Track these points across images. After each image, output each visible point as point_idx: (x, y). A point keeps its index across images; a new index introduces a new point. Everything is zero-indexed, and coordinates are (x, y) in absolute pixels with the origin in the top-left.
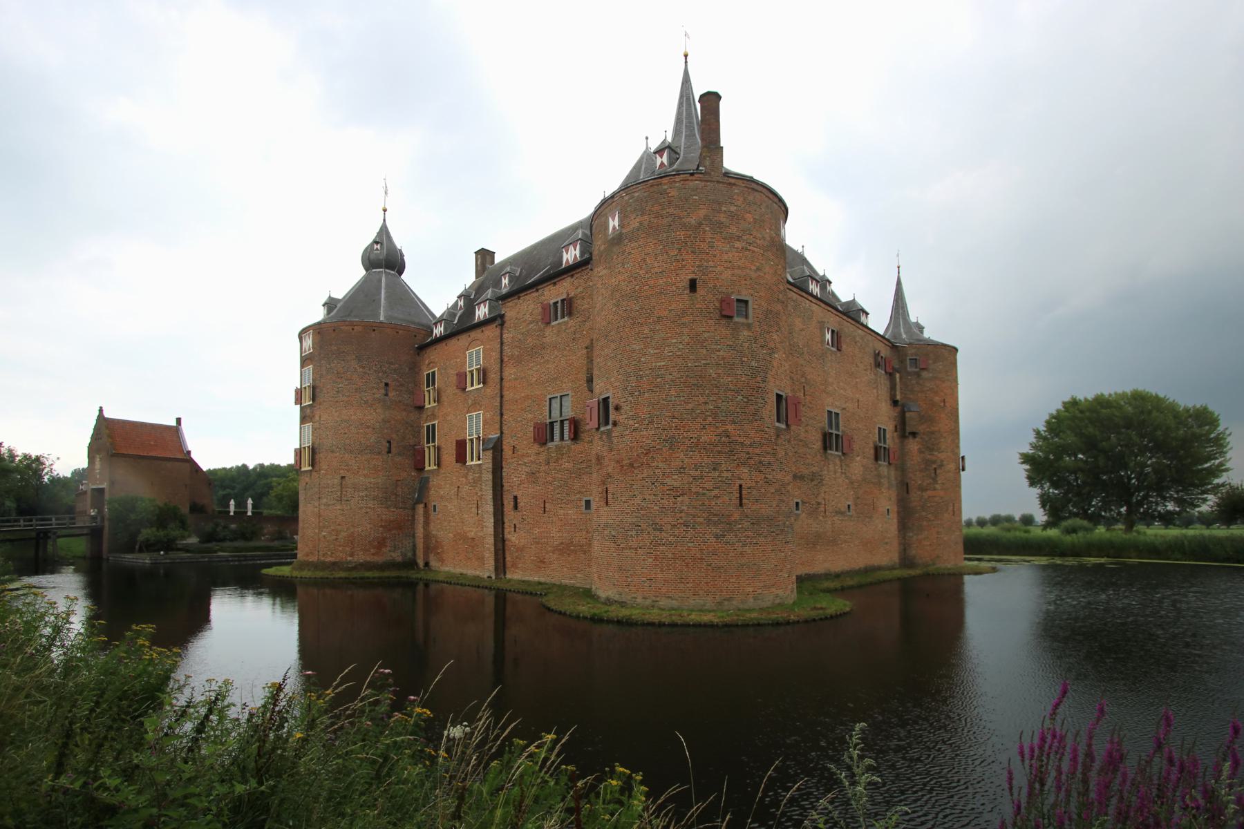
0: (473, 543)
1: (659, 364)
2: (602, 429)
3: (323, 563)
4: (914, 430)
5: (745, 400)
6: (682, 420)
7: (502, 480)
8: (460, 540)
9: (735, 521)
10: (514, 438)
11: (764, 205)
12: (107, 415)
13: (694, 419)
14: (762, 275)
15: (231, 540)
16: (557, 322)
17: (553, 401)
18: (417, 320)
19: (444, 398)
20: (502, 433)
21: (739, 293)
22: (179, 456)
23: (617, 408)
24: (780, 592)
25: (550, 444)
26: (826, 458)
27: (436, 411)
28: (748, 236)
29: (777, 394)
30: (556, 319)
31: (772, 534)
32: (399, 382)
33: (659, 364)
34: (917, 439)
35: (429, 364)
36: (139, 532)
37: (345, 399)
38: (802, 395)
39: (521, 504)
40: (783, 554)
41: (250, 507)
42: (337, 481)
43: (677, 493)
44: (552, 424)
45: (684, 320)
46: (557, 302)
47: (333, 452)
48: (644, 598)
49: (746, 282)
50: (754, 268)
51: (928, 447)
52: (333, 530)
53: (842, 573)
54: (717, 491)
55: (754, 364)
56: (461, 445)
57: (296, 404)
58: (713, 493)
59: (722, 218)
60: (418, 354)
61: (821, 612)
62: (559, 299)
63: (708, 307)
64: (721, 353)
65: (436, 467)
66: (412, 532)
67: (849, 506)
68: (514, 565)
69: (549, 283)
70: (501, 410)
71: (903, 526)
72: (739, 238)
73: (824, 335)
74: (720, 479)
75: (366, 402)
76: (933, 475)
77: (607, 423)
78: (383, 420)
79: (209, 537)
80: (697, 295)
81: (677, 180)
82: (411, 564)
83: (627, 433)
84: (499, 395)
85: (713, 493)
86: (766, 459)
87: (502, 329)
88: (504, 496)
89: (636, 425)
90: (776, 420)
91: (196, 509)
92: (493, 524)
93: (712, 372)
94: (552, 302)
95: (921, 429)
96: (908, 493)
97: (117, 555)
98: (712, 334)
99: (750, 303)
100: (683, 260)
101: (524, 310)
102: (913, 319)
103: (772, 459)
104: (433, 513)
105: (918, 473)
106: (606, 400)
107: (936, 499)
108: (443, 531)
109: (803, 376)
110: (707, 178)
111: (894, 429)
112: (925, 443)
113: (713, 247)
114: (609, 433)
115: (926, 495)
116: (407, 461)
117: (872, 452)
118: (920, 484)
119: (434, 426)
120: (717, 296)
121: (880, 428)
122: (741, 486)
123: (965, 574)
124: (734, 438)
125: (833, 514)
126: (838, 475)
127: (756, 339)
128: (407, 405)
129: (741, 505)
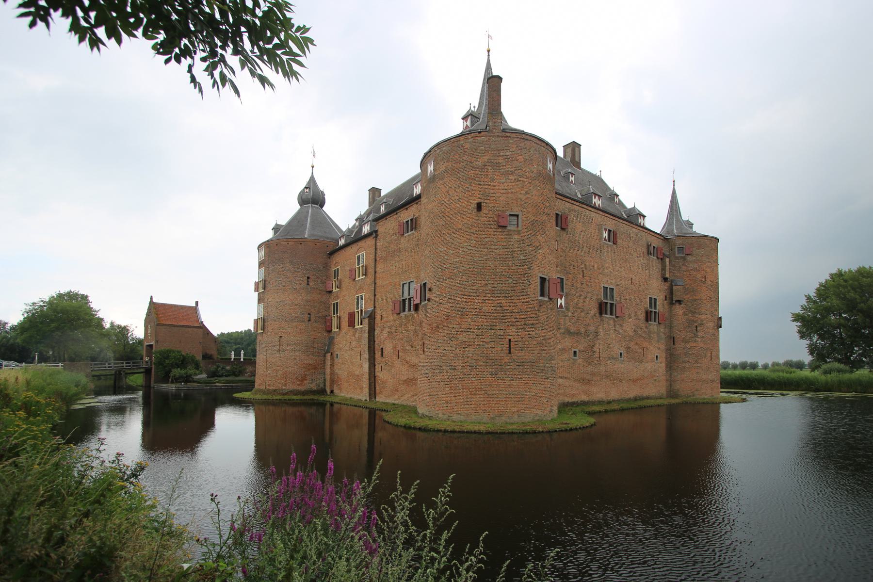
0: (358, 378)
1: (455, 260)
2: (422, 303)
3: (268, 390)
5: (515, 282)
6: (470, 296)
7: (374, 338)
8: (351, 376)
9: (505, 363)
10: (382, 310)
11: (533, 149)
12: (155, 300)
13: (478, 296)
14: (530, 196)
15: (226, 376)
16: (408, 234)
17: (405, 285)
18: (329, 236)
19: (343, 285)
20: (375, 307)
22: (196, 325)
23: (430, 290)
24: (540, 412)
25: (402, 314)
26: (601, 320)
27: (339, 294)
29: (540, 277)
30: (408, 232)
31: (534, 372)
32: (316, 276)
33: (455, 260)
35: (336, 264)
36: (170, 371)
37: (283, 288)
38: (581, 277)
39: (385, 353)
40: (542, 386)
41: (242, 355)
42: (277, 339)
43: (465, 345)
44: (404, 301)
45: (473, 230)
46: (408, 221)
47: (275, 321)
48: (443, 414)
49: (517, 202)
50: (523, 192)
52: (274, 370)
53: (614, 401)
54: (492, 344)
55: (522, 257)
56: (352, 316)
57: (255, 291)
58: (490, 345)
60: (329, 258)
61: (564, 426)
62: (409, 219)
65: (338, 330)
66: (323, 371)
68: (381, 392)
69: (404, 209)
70: (374, 293)
74: (495, 335)
75: (295, 289)
77: (425, 301)
79: (214, 374)
80: (481, 212)
81: (469, 137)
82: (322, 391)
83: (436, 306)
84: (373, 283)
85: (490, 345)
87: (376, 240)
88: (376, 348)
89: (441, 301)
90: (539, 295)
91: (206, 357)
92: (368, 366)
93: (491, 264)
94: (405, 221)
95: (686, 297)
97: (159, 385)
98: (492, 239)
99: (519, 216)
100: (472, 190)
101: (389, 226)
104: (336, 359)
106: (425, 284)
108: (341, 371)
111: (664, 298)
114: (426, 306)
116: (321, 326)
119: (337, 303)
120: (495, 213)
122: (510, 340)
123: (721, 403)
127: (523, 241)
129: (510, 352)
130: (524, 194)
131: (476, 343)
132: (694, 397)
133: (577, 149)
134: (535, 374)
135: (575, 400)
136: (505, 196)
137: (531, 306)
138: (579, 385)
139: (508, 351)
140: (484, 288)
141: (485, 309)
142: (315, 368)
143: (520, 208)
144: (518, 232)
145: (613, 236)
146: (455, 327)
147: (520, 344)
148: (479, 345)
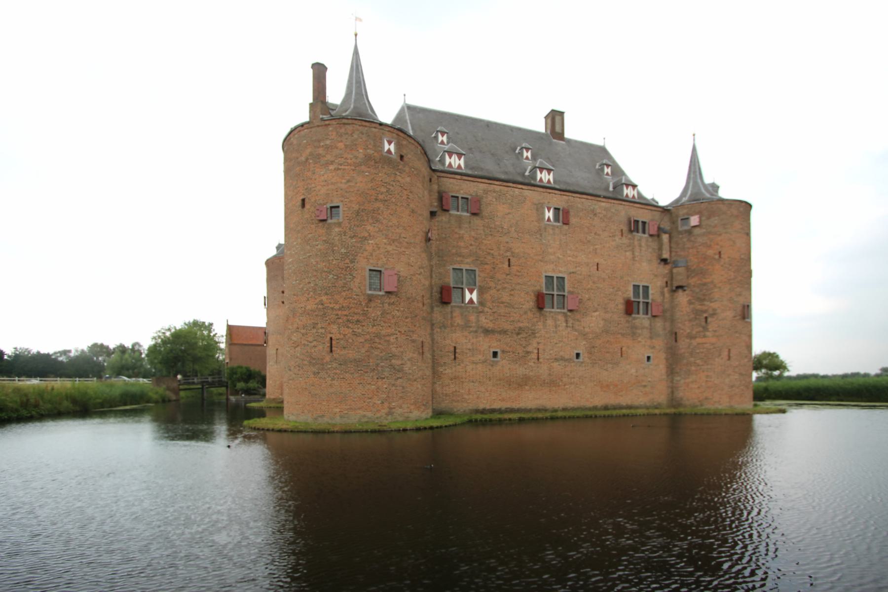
4: (681, 284)
5: (335, 277)
6: (297, 296)
9: (327, 363)
13: (303, 294)
21: (332, 201)
28: (339, 159)
34: (687, 292)
54: (315, 343)
55: (343, 251)
59: (321, 151)
63: (311, 217)
67: (578, 355)
72: (332, 163)
73: (543, 214)
76: (703, 324)
85: (313, 344)
86: (356, 317)
103: (361, 318)
105: (686, 323)
107: (705, 346)
109: (507, 251)
113: (314, 173)
115: (694, 342)
117: (622, 307)
118: (689, 333)
121: (636, 287)
122: (331, 339)
124: (326, 305)
125: (552, 361)
126: (561, 328)
127: (345, 233)
129: (331, 351)
130: (346, 183)
131: (303, 343)
132: (703, 407)
133: (558, 118)
134: (361, 373)
135: (496, 406)
136: (325, 188)
137: (356, 301)
138: (502, 390)
139: (329, 349)
141: (309, 307)
143: (340, 199)
144: (339, 224)
147: (342, 342)
148: (304, 345)
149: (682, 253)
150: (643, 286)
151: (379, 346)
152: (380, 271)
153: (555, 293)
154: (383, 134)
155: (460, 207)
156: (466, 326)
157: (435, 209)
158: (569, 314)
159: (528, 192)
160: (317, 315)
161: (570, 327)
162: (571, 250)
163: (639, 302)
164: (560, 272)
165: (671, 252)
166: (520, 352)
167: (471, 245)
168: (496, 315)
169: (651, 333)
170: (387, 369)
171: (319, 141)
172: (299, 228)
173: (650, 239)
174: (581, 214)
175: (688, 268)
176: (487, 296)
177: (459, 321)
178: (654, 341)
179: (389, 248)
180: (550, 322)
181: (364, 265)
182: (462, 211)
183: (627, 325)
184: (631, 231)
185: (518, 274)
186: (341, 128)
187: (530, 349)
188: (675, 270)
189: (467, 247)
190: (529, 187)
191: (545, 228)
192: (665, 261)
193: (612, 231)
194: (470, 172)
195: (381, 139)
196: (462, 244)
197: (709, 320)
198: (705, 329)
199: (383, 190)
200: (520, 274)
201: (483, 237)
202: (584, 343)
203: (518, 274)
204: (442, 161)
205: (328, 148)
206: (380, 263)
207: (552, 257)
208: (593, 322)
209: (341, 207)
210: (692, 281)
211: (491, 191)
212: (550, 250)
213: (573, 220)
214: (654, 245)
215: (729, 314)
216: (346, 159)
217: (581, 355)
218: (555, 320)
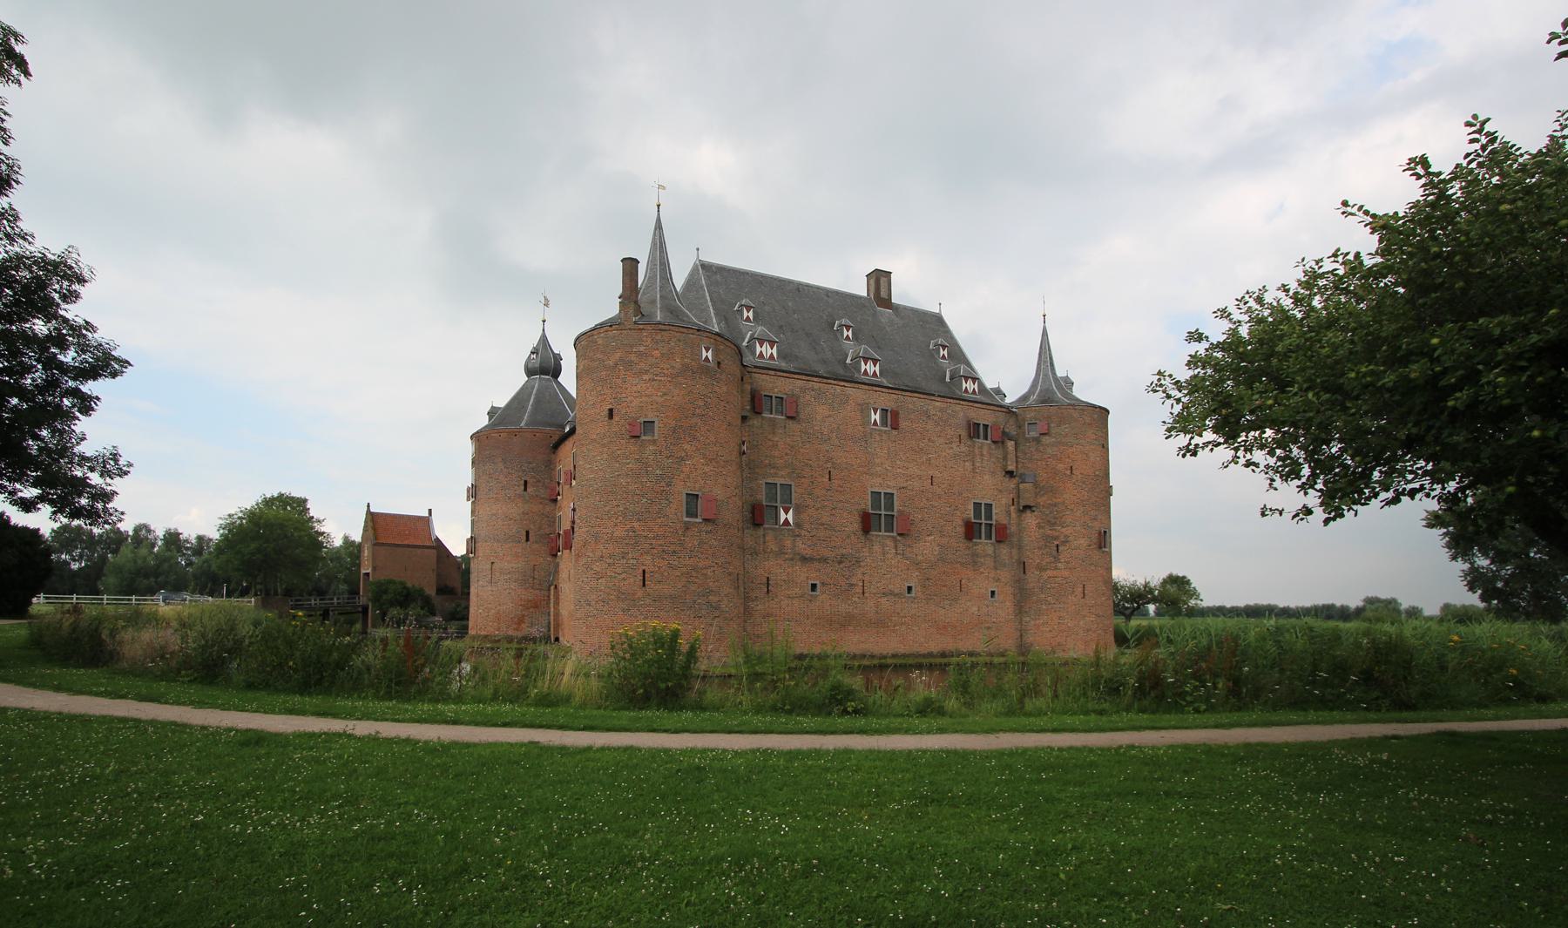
4: (1028, 503)
9: (639, 598)
34: (1036, 513)
42: (489, 566)
43: (599, 576)
51: (1049, 521)
54: (623, 576)
55: (658, 472)
58: (623, 576)
59: (633, 357)
64: (630, 465)
67: (910, 589)
71: (1020, 610)
72: (647, 372)
73: (870, 416)
75: (509, 498)
76: (1055, 553)
78: (523, 513)
85: (623, 576)
86: (672, 548)
96: (1024, 572)
102: (1060, 373)
103: (678, 548)
110: (622, 327)
112: (1044, 517)
117: (961, 530)
121: (977, 506)
122: (644, 571)
126: (890, 556)
128: (543, 498)
129: (644, 585)
130: (661, 396)
140: (616, 509)
142: (536, 607)
144: (654, 442)
145: (892, 419)
146: (591, 555)
149: (1030, 465)
150: (985, 504)
151: (697, 580)
152: (697, 495)
153: (883, 512)
154: (701, 340)
155: (774, 409)
156: (781, 553)
157: (745, 414)
158: (899, 538)
159: (851, 391)
160: (627, 544)
161: (899, 554)
162: (901, 459)
163: (981, 524)
164: (888, 487)
165: (1017, 462)
166: (843, 584)
167: (787, 454)
168: (814, 539)
169: (995, 562)
170: (704, 607)
171: (632, 346)
172: (605, 441)
173: (993, 446)
174: (912, 417)
175: (1036, 484)
176: (804, 516)
177: (773, 546)
178: (998, 572)
179: (707, 469)
180: (877, 548)
181: (681, 490)
182: (776, 414)
183: (967, 552)
184: (970, 437)
185: (839, 489)
186: (657, 334)
187: (854, 581)
188: (1021, 486)
189: (781, 457)
190: (852, 385)
191: (871, 434)
192: (1010, 474)
193: (949, 437)
194: (784, 365)
195: (699, 346)
196: (776, 453)
197: (1061, 548)
198: (1057, 559)
199: (701, 403)
200: (842, 489)
201: (800, 445)
202: (917, 573)
203: (839, 489)
204: (751, 348)
205: (640, 354)
206: (697, 486)
207: (878, 469)
208: (927, 548)
209: (656, 423)
210: (1042, 500)
211: (808, 389)
212: (877, 461)
213: (903, 424)
214: (998, 453)
215: (1083, 542)
216: (662, 369)
217: (913, 588)
218: (884, 545)
